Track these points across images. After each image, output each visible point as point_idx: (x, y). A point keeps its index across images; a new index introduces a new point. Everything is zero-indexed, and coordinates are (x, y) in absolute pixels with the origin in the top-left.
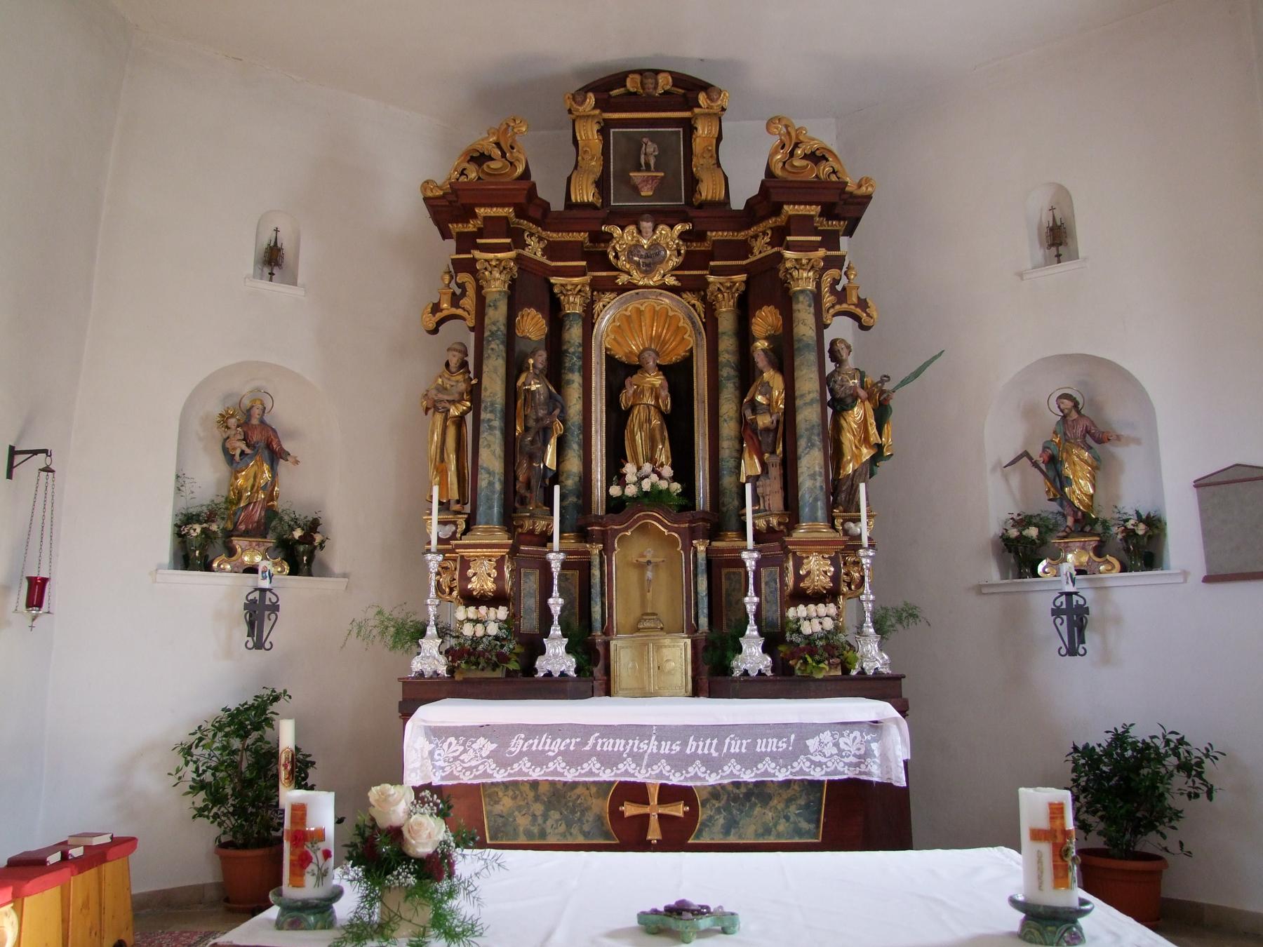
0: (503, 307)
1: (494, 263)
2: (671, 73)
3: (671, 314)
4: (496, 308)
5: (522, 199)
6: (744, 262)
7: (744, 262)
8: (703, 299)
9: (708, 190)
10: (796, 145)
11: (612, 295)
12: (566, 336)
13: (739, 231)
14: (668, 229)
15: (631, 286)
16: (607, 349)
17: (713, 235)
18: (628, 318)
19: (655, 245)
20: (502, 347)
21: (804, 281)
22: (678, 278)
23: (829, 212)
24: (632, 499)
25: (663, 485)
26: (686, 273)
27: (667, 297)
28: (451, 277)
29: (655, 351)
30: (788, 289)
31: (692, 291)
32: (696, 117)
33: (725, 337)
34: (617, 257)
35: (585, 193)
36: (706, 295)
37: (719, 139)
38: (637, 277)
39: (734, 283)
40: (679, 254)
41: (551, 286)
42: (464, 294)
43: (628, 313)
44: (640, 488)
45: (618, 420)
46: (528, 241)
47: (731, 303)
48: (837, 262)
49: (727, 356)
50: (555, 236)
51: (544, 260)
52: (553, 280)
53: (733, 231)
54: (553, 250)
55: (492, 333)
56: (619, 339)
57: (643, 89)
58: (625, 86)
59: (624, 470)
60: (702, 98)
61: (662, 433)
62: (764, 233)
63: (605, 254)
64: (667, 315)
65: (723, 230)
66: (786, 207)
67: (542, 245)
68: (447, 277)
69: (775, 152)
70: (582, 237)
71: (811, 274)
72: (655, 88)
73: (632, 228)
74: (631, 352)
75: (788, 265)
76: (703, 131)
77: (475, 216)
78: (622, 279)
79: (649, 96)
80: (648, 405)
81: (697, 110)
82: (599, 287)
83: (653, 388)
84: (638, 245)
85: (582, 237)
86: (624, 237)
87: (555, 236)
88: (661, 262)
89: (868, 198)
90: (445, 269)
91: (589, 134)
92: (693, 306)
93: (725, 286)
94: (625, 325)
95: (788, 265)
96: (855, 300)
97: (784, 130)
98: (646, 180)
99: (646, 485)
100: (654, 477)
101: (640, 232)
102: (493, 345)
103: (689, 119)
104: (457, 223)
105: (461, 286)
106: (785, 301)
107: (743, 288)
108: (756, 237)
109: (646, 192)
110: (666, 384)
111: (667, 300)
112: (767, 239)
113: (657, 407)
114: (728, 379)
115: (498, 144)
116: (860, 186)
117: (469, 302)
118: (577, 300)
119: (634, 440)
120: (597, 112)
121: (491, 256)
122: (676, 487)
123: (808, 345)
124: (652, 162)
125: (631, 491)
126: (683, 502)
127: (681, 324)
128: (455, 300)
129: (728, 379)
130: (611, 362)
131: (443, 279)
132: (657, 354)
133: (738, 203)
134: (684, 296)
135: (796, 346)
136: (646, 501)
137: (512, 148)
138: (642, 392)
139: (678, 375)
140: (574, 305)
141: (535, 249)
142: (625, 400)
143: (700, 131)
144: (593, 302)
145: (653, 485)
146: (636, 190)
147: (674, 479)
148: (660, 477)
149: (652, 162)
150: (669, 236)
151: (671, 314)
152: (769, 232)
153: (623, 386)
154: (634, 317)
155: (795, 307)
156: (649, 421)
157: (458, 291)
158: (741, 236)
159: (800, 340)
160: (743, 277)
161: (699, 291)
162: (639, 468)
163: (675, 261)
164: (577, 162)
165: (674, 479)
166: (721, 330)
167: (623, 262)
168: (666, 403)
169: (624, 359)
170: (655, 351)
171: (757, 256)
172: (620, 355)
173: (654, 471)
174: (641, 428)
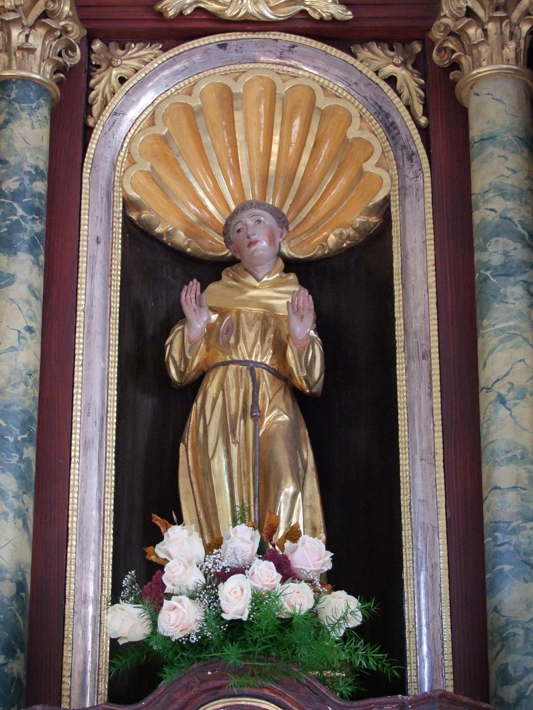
3: (323, 102)
8: (421, 64)
11: (147, 52)
16: (128, 204)
18: (191, 114)
24: (182, 646)
25: (297, 599)
27: (306, 57)
29: (277, 214)
31: (389, 38)
43: (195, 102)
44: (214, 613)
45: (158, 408)
47: (510, 51)
49: (500, 204)
56: (162, 172)
59: (160, 551)
61: (295, 450)
64: (312, 106)
74: (207, 221)
80: (252, 367)
83: (268, 321)
92: (391, 80)
94: (183, 130)
99: (235, 601)
100: (265, 573)
110: (306, 300)
111: (314, 68)
113: (282, 375)
114: (505, 271)
118: (36, 40)
119: (204, 473)
122: (343, 608)
125: (181, 618)
126: (368, 658)
127: (353, 133)
129: (505, 271)
130: (139, 238)
132: (282, 221)
134: (364, 53)
136: (232, 654)
138: (235, 329)
139: (348, 285)
142: (182, 352)
144: (90, 67)
145: (258, 600)
147: (334, 580)
148: (286, 571)
151: (323, 102)
153: (176, 316)
154: (214, 113)
156: (253, 411)
161: (406, 41)
162: (214, 544)
165: (334, 580)
166: (477, 129)
168: (309, 363)
169: (181, 238)
170: (277, 214)
172: (170, 224)
173: (263, 552)
174: (227, 430)
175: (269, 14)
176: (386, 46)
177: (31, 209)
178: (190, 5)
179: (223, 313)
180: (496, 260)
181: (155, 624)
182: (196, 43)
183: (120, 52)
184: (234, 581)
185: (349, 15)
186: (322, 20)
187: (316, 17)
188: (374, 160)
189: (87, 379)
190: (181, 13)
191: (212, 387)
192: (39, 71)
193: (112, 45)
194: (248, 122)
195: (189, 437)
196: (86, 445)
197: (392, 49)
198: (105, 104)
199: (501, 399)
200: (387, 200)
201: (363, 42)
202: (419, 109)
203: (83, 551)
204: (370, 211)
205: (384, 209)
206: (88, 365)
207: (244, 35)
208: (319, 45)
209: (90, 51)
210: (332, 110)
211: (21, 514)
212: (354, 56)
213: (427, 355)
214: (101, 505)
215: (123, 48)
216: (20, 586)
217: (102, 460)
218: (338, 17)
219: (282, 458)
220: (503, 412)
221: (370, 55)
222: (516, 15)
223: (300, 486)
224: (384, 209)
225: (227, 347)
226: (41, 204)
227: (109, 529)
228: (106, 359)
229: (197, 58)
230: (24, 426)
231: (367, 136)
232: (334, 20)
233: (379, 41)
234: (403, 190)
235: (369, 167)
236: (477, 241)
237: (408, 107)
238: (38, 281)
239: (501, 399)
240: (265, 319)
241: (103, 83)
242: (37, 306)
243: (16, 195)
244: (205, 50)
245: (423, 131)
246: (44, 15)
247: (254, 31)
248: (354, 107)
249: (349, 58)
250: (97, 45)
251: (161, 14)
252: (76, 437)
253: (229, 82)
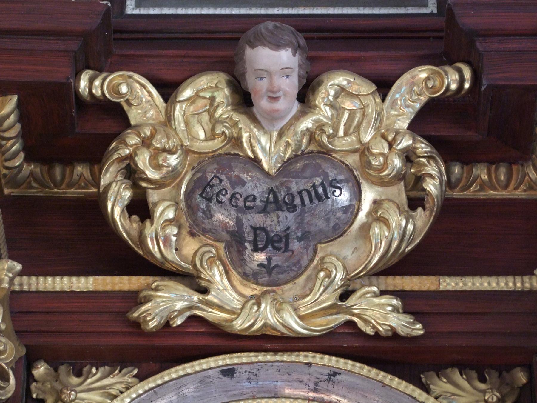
14: (365, 88)
15: (201, 339)
19: (315, 155)
22: (410, 303)
26: (449, 284)
34: (140, 208)
38: (229, 299)
40: (415, 203)
63: (95, 206)
73: (206, 88)
78: (167, 303)
84: (232, 158)
86: (172, 124)
88: (338, 232)
101: (244, 100)
161: (504, 368)
167: (163, 236)
175: (298, 327)
176: (474, 374)
178: (181, 312)
182: (188, 368)
183: (75, 380)
185: (418, 329)
186: (377, 334)
187: (369, 331)
190: (167, 324)
193: (63, 369)
197: (483, 380)
201: (440, 368)
207: (261, 357)
208: (374, 372)
209: (30, 378)
212: (426, 389)
215: (78, 374)
218: (402, 331)
221: (449, 387)
229: (189, 390)
232: (395, 335)
233: (462, 367)
244: (203, 378)
247: (276, 351)
249: (418, 393)
250: (41, 370)
251: (137, 325)
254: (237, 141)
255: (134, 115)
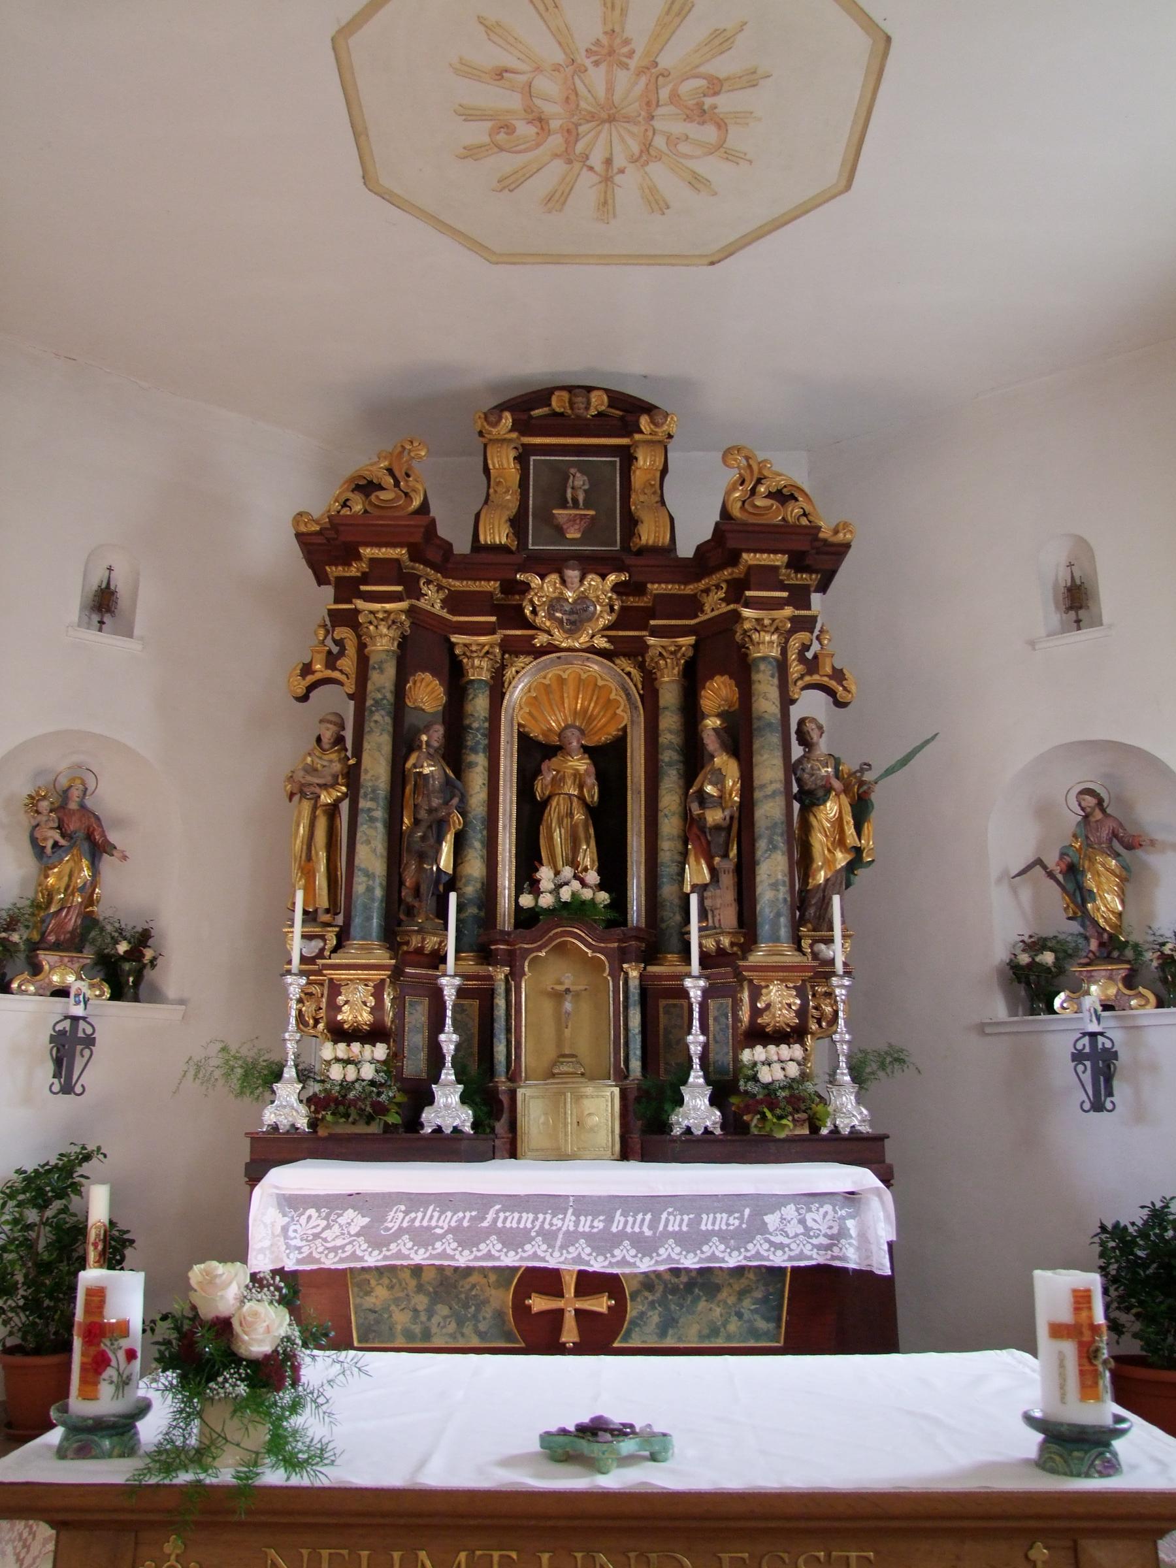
0: (391, 670)
1: (380, 615)
2: (606, 390)
3: (600, 683)
4: (382, 671)
5: (417, 538)
6: (692, 622)
7: (692, 622)
8: (641, 666)
9: (649, 534)
10: (759, 481)
11: (528, 659)
12: (469, 708)
13: (686, 583)
14: (599, 579)
15: (551, 649)
16: (519, 725)
17: (655, 588)
19: (582, 598)
20: (388, 720)
21: (767, 645)
22: (610, 639)
23: (798, 563)
24: (549, 911)
25: (587, 894)
26: (621, 633)
27: (596, 663)
28: (327, 632)
30: (746, 655)
32: (636, 444)
33: (667, 713)
34: (534, 612)
35: (497, 533)
36: (644, 661)
37: (664, 471)
38: (560, 638)
39: (680, 647)
40: (612, 610)
41: (452, 646)
42: (342, 653)
43: (547, 682)
44: (558, 898)
45: (532, 812)
46: (425, 589)
47: (676, 671)
48: (806, 624)
50: (458, 585)
51: (444, 614)
52: (454, 638)
53: (679, 583)
54: (454, 602)
55: (377, 703)
57: (572, 408)
58: (550, 405)
59: (538, 875)
60: (644, 422)
62: (718, 587)
63: (520, 609)
65: (667, 582)
66: (745, 556)
67: (442, 595)
68: (322, 632)
69: (733, 489)
70: (492, 586)
71: (775, 637)
72: (587, 408)
73: (554, 577)
74: (551, 730)
75: (747, 626)
76: (645, 461)
77: (358, 557)
78: (541, 639)
79: (578, 417)
80: (570, 795)
81: (637, 437)
82: (511, 648)
84: (562, 599)
85: (492, 586)
86: (543, 588)
87: (458, 585)
88: (590, 620)
89: (847, 546)
90: (319, 621)
91: (504, 462)
92: (629, 674)
93: (668, 651)
94: (541, 696)
95: (747, 626)
96: (829, 670)
97: (744, 462)
98: (573, 520)
99: (565, 894)
100: (576, 885)
101: (563, 582)
102: (377, 717)
103: (628, 447)
104: (336, 565)
105: (339, 643)
106: (742, 670)
107: (690, 653)
108: (707, 591)
109: (573, 534)
110: (592, 770)
111: (596, 667)
112: (721, 594)
113: (581, 798)
114: (670, 764)
115: (390, 471)
116: (836, 532)
117: (348, 663)
118: (484, 664)
119: (550, 838)
120: (514, 435)
121: (378, 606)
122: (603, 897)
123: (770, 725)
124: (581, 498)
125: (546, 901)
126: (611, 915)
127: (613, 696)
128: (331, 661)
129: (670, 764)
131: (316, 634)
132: (582, 732)
133: (686, 549)
134: (618, 661)
135: (755, 726)
136: (565, 913)
137: (408, 475)
138: (563, 779)
139: (608, 759)
140: (479, 670)
141: (432, 600)
142: (540, 788)
143: (641, 462)
144: (503, 667)
145: (574, 894)
146: (560, 531)
147: (601, 887)
148: (584, 884)
149: (581, 498)
150: (599, 588)
151: (600, 683)
152: (724, 586)
153: (538, 772)
154: (555, 686)
155: (755, 677)
156: (571, 815)
157: (335, 650)
158: (689, 589)
159: (760, 718)
160: (691, 640)
161: (636, 656)
162: (557, 873)
163: (606, 619)
164: (488, 495)
165: (601, 887)
167: (542, 619)
168: (593, 794)
169: (541, 738)
171: (708, 614)
173: (576, 877)
177: (483, 735)
179: (558, 772)
180: (667, 759)
181: (537, 902)
184: (565, 888)
188: (622, 708)
189: (504, 800)
191: (554, 803)
192: (485, 676)
194: (570, 689)
195: (544, 823)
196: (504, 827)
198: (510, 683)
199: (666, 816)
200: (625, 727)
201: (618, 656)
202: (640, 686)
203: (504, 870)
204: (618, 730)
205: (625, 729)
206: (505, 795)
210: (604, 686)
211: (482, 857)
213: (639, 792)
214: (510, 851)
216: (483, 884)
217: (510, 833)
219: (582, 835)
220: (666, 821)
222: (679, 655)
223: (588, 846)
224: (625, 729)
225: (560, 787)
226: (487, 732)
227: (514, 860)
228: (511, 792)
230: (483, 823)
231: (619, 698)
233: (624, 656)
234: (632, 722)
235: (619, 711)
236: (660, 750)
237: (635, 686)
238: (486, 764)
239: (666, 816)
240: (575, 775)
241: (510, 672)
242: (486, 773)
243: (478, 730)
244: (552, 660)
245: (641, 696)
246: (488, 652)
248: (613, 685)
250: (507, 656)
251: (534, 645)
252: (500, 824)
253: (561, 673)
254: (562, 593)
255: (533, 585)
